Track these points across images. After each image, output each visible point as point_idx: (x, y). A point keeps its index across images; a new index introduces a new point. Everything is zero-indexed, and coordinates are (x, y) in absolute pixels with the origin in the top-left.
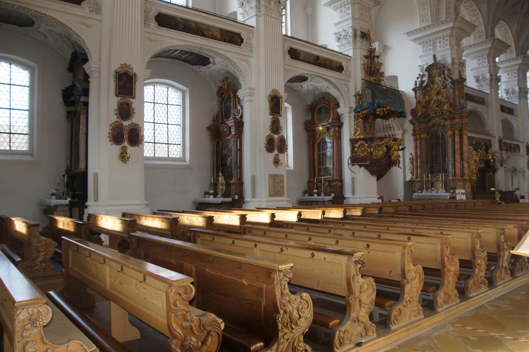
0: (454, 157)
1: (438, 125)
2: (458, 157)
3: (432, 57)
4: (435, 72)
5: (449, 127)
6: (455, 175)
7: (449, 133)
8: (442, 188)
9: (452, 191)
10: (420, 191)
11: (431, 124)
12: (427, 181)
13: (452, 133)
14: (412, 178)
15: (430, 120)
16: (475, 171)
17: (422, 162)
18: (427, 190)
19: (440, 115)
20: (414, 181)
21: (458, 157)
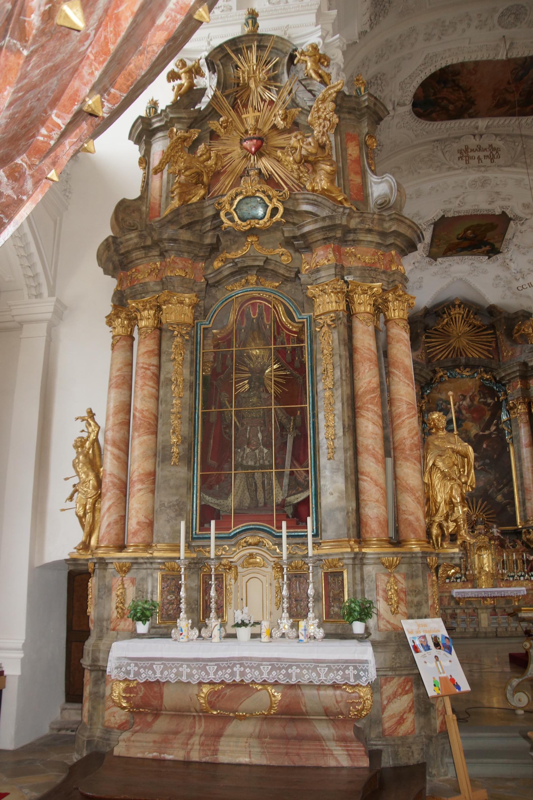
0: (352, 429)
1: (264, 270)
2: (370, 428)
3: (243, 14)
4: (249, 65)
5: (327, 275)
6: (358, 530)
7: (328, 303)
8: (297, 613)
9: (358, 627)
10: (142, 628)
11: (217, 264)
12: (197, 565)
13: (342, 306)
14: (85, 546)
15: (214, 249)
16: (460, 511)
17: (160, 454)
18: (199, 624)
19: (278, 223)
20: (103, 563)
21: (370, 428)
